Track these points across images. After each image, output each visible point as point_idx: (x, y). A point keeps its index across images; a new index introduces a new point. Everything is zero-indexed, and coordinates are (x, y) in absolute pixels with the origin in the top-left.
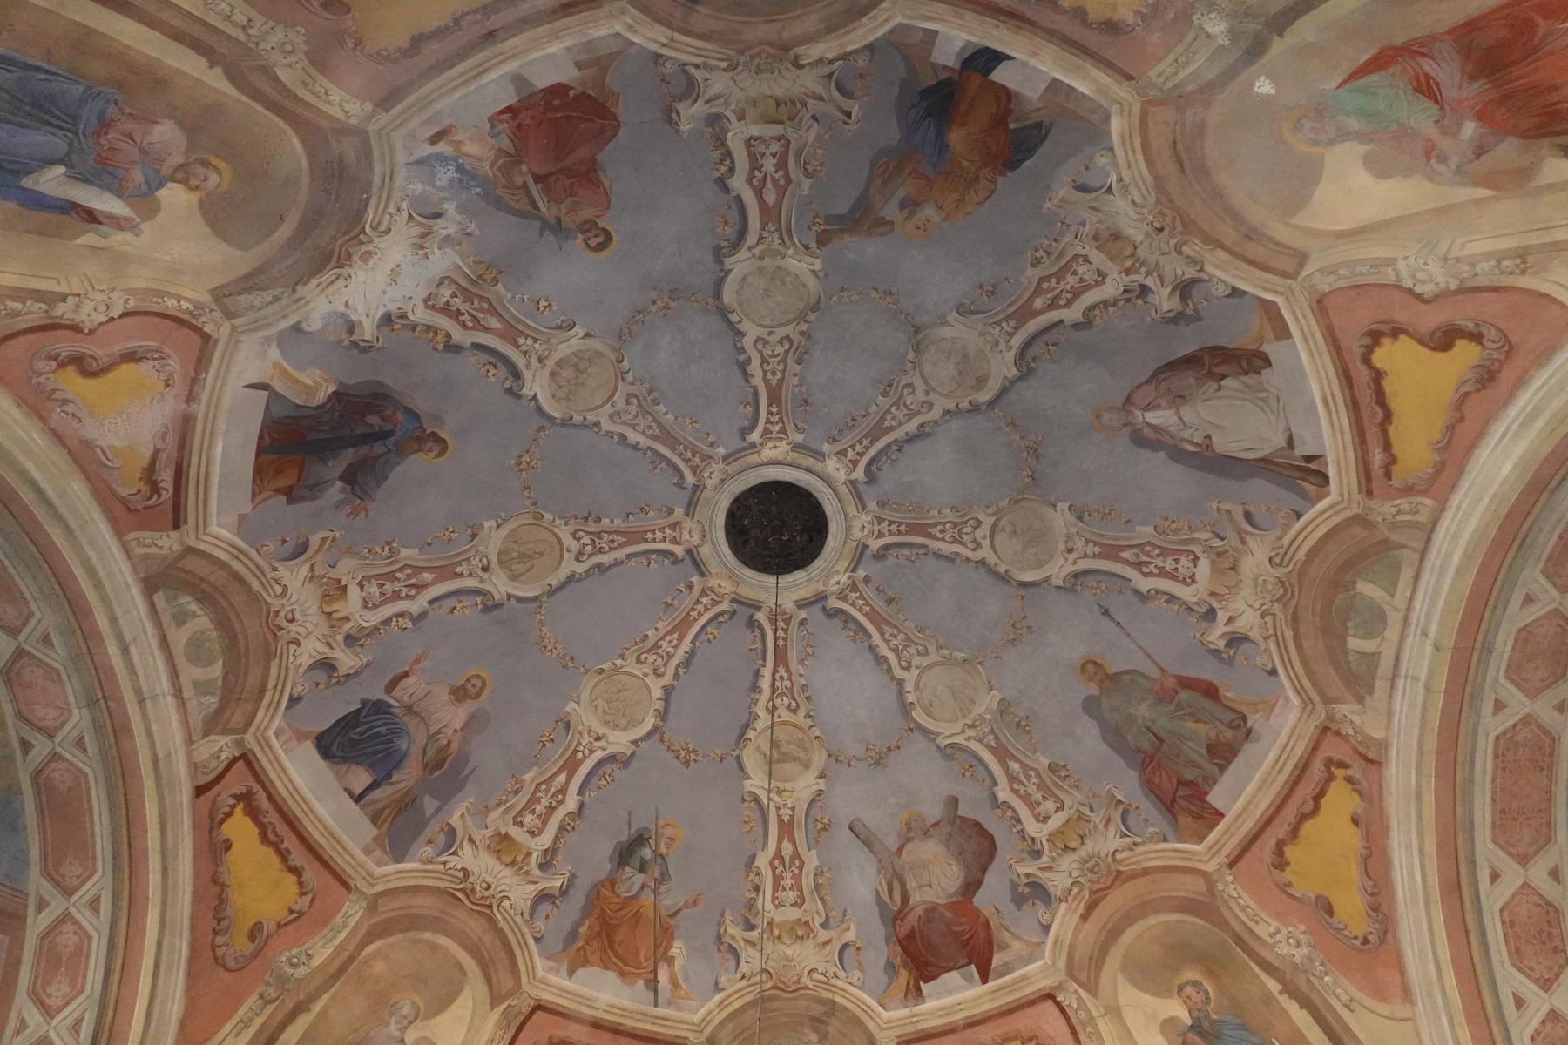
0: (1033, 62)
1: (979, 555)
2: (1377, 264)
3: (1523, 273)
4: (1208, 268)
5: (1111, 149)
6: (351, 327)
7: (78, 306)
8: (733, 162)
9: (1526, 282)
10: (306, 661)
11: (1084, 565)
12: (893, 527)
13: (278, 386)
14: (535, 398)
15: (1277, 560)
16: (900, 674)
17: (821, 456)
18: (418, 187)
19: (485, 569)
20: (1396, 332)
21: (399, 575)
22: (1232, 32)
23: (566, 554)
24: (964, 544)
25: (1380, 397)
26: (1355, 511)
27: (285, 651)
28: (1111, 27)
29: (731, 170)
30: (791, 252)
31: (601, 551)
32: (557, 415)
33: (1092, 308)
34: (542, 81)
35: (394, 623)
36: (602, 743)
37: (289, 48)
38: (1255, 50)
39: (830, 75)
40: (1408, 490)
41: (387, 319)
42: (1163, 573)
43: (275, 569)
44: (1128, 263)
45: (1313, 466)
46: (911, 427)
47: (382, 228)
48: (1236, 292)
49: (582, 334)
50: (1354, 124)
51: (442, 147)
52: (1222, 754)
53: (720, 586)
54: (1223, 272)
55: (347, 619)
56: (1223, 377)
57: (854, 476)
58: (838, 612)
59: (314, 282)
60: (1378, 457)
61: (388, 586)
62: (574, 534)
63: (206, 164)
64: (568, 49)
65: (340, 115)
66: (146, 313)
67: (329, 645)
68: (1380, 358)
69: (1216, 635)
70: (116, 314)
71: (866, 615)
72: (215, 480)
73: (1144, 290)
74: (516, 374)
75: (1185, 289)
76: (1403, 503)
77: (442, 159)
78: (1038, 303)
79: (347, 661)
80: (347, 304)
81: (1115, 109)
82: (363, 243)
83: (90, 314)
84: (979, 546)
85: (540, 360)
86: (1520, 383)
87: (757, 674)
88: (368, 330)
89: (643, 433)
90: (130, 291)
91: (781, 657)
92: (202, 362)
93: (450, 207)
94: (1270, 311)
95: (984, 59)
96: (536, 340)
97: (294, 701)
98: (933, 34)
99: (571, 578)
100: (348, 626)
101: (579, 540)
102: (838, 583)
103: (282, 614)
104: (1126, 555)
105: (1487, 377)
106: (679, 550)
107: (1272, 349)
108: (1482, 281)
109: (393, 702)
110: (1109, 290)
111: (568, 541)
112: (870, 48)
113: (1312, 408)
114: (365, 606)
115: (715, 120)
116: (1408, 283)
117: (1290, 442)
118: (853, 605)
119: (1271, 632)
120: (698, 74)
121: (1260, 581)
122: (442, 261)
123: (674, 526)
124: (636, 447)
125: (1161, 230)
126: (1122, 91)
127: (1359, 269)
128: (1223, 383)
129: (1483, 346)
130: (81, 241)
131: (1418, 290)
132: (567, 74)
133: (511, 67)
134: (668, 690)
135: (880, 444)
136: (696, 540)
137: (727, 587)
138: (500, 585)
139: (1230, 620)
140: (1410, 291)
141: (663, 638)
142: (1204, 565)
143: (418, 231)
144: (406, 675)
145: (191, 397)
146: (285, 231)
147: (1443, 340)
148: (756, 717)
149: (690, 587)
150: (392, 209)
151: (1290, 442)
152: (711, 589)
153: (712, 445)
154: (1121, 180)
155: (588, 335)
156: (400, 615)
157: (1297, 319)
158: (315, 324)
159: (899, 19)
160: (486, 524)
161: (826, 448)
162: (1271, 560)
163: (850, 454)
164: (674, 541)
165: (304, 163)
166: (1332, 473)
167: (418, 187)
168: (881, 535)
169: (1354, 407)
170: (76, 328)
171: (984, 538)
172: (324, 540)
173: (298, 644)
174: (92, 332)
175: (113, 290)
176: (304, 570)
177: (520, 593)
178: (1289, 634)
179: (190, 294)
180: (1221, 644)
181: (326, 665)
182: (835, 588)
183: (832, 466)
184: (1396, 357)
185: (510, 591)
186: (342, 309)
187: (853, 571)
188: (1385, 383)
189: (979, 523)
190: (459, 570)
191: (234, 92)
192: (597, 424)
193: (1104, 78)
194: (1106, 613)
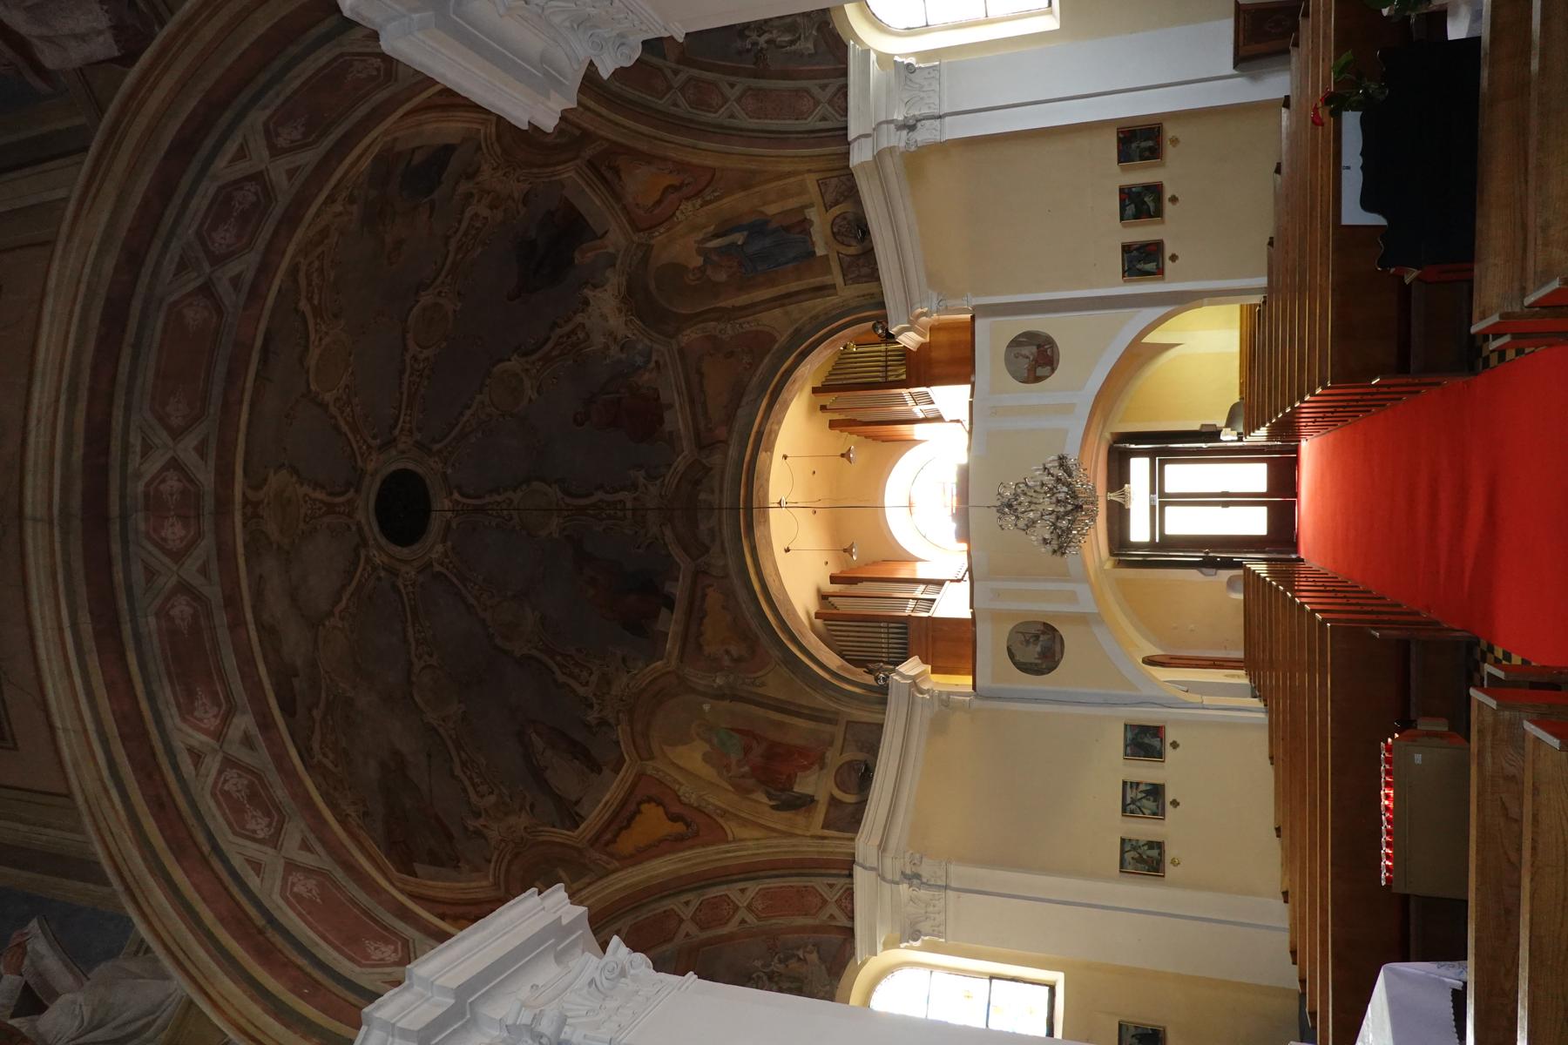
0: (673, 622)
1: (415, 660)
2: (675, 780)
3: (722, 817)
4: (619, 727)
5: (647, 666)
6: (595, 287)
7: (694, 206)
8: (611, 494)
9: (721, 821)
10: (485, 167)
11: (441, 730)
12: (411, 595)
13: (598, 242)
14: (509, 360)
15: (529, 830)
16: (337, 610)
17: (444, 541)
18: (640, 347)
19: (440, 292)
20: (660, 804)
21: (472, 241)
22: (720, 687)
23: (419, 349)
24: (417, 649)
25: (631, 819)
26: (579, 845)
27: (497, 160)
28: (700, 647)
29: (607, 492)
30: (561, 521)
31: (411, 374)
32: (495, 369)
33: (569, 685)
34: (667, 415)
35: (456, 224)
36: (316, 343)
37: (723, 332)
38: (722, 697)
39: (657, 539)
40: (611, 855)
41: (586, 303)
42: (470, 779)
43: (530, 183)
44: (599, 694)
45: (577, 818)
46: (472, 601)
47: (629, 323)
48: (617, 743)
49: (533, 397)
50: (715, 741)
51: (652, 365)
52: (435, 859)
53: (372, 460)
54: (622, 733)
55: (479, 201)
56: (577, 759)
57: (435, 564)
58: (358, 556)
59: (625, 283)
60: (608, 836)
61: (474, 232)
62: (427, 359)
63: (698, 279)
64: (679, 430)
65: (685, 333)
66: (667, 220)
67: (477, 183)
68: (644, 807)
69: (472, 824)
70: (678, 213)
71: (360, 581)
72: (587, 190)
73: (591, 706)
74: (525, 354)
75: (603, 722)
76: (605, 858)
77: (648, 362)
78: (558, 658)
79: (464, 187)
80: (606, 290)
81: (665, 661)
82: (627, 311)
83: (687, 207)
84: (420, 657)
85: (527, 370)
86: (691, 847)
87: (323, 487)
88: (588, 292)
89: (468, 421)
90: (679, 223)
91: (331, 509)
92: (632, 222)
93: (623, 356)
94: (620, 762)
95: (670, 603)
96: (538, 371)
97: (479, 148)
98: (677, 580)
99: (405, 348)
100: (476, 198)
101: (423, 361)
102: (374, 555)
103: (512, 172)
104: (463, 754)
105: (680, 839)
106: (396, 432)
107: (606, 772)
108: (707, 811)
109: (426, 200)
110: (581, 691)
111: (426, 353)
112: (670, 555)
113: (599, 801)
114: (476, 215)
115: (635, 487)
116: (680, 793)
117: (577, 803)
118: (364, 569)
119: (501, 848)
120: (658, 482)
121: (512, 829)
122: (598, 340)
123: (410, 431)
124: (461, 414)
125: (623, 701)
126: (674, 662)
127: (668, 777)
128: (575, 761)
129: (687, 829)
130: (712, 227)
131: (682, 798)
132: (667, 427)
133: (677, 405)
134: (324, 406)
135: (455, 580)
136: (401, 446)
137: (371, 467)
138: (426, 298)
139: (485, 826)
140: (679, 797)
141: (352, 411)
142: (492, 799)
143: (619, 337)
144: (430, 217)
145: (624, 208)
146: (652, 286)
147: (675, 818)
148: (302, 484)
149: (374, 437)
150: (635, 332)
151: (577, 803)
152: (370, 454)
153: (453, 465)
154: (636, 675)
155: (530, 400)
156: (457, 230)
157: (627, 771)
158: (609, 273)
159: (682, 565)
160: (460, 304)
161: (449, 544)
162: (525, 828)
163: (447, 561)
164: (402, 430)
165: (675, 310)
166: (582, 826)
167: (640, 347)
168: (406, 586)
169: (616, 814)
170: (688, 199)
171: (425, 662)
172: (518, 213)
173: (493, 169)
174: (681, 201)
175: (686, 219)
176: (516, 195)
177: (415, 310)
178: (508, 857)
179: (659, 237)
180: (471, 829)
181: (470, 177)
182: (371, 554)
183: (440, 548)
184: (652, 813)
185: (419, 304)
186: (606, 287)
187: (383, 568)
188: (637, 818)
189: (431, 656)
190: (450, 277)
191: (718, 305)
192: (481, 393)
193: (676, 652)
194: (429, 756)
